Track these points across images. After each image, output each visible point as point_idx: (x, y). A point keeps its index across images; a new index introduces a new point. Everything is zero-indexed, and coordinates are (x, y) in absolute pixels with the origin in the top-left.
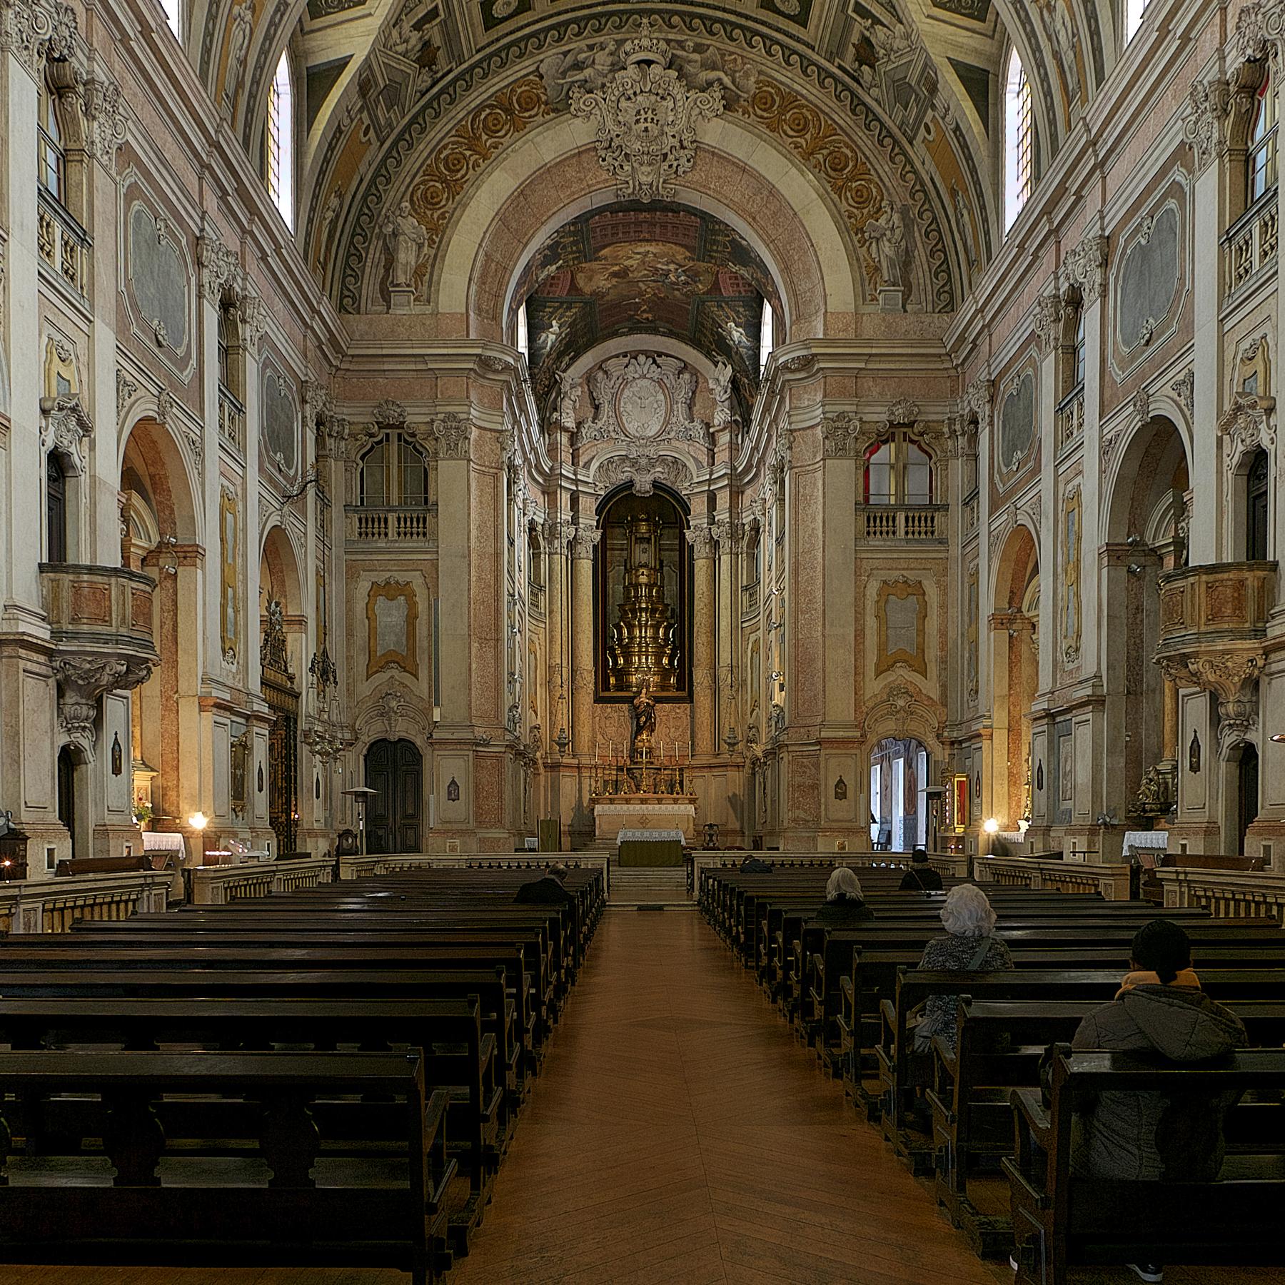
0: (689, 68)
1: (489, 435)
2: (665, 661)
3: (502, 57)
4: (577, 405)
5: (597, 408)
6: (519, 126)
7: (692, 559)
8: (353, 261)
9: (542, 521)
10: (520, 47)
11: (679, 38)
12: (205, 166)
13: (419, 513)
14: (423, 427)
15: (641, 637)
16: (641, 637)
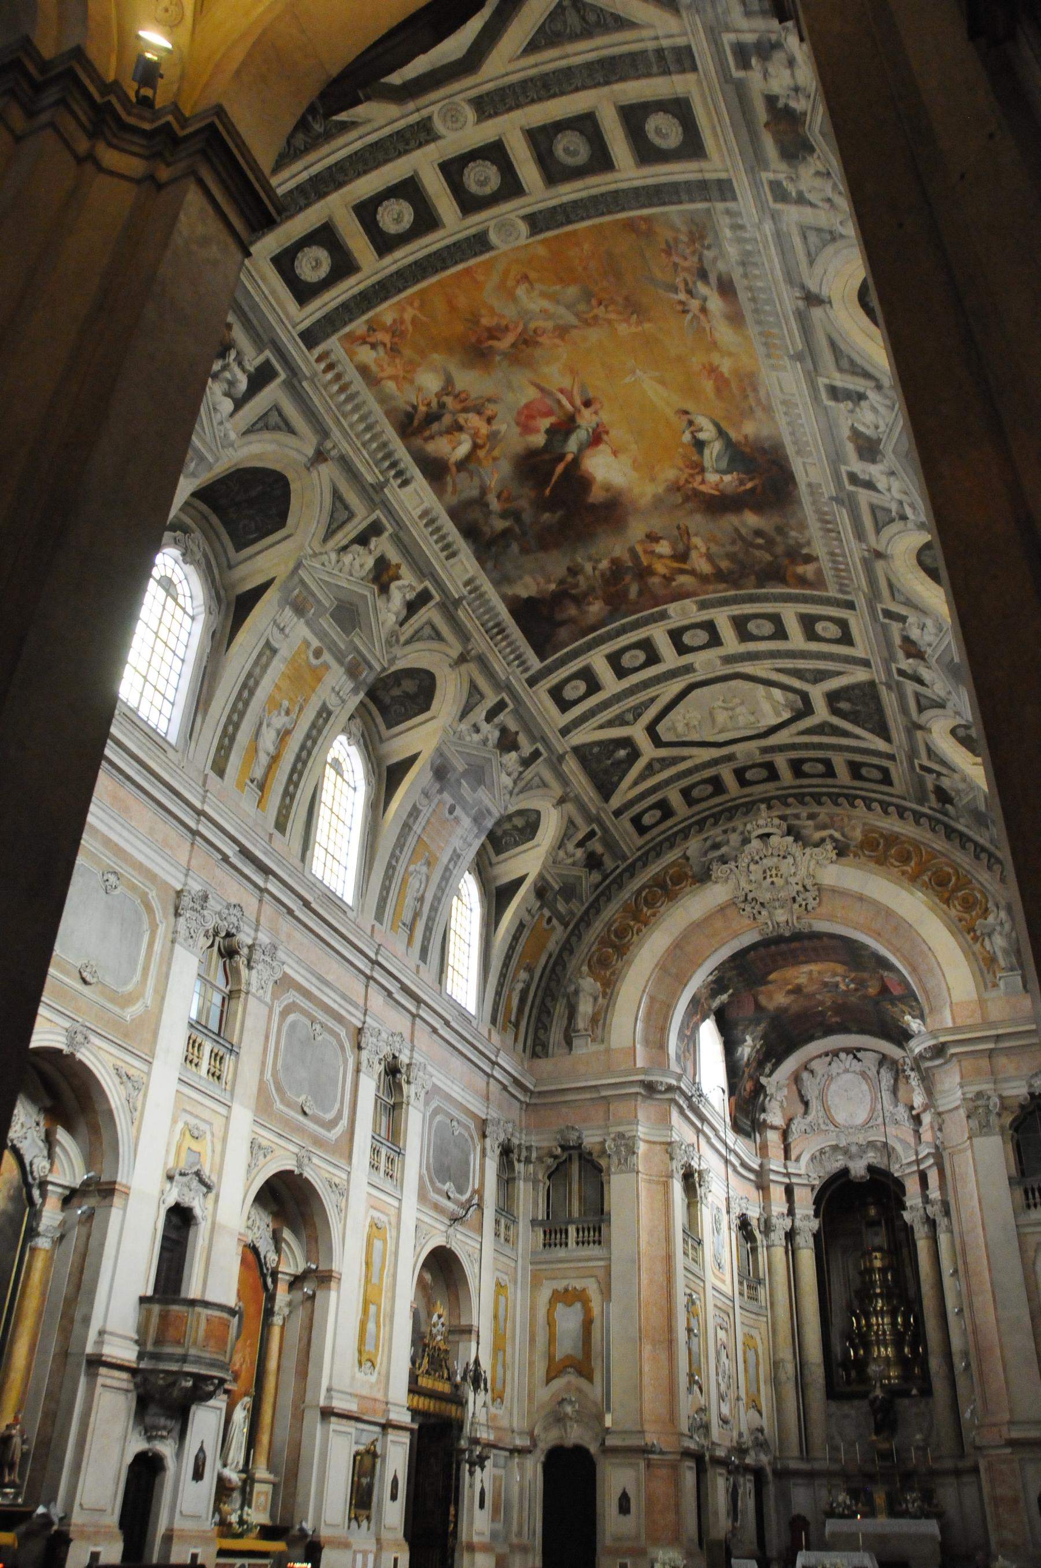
0: (805, 832)
1: (658, 1147)
3: (657, 850)
4: (785, 1104)
5: (806, 1104)
6: (671, 895)
8: (544, 1018)
9: (757, 1215)
10: (671, 842)
11: (795, 811)
12: (369, 978)
13: (596, 1223)
14: (598, 1147)
16: (878, 1325)
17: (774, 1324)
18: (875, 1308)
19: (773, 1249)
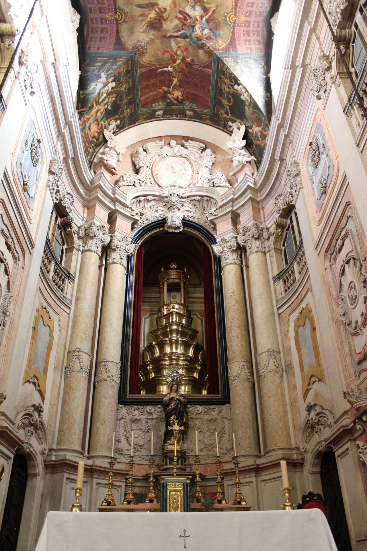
2: (196, 375)
7: (220, 269)
15: (172, 353)
17: (75, 316)
18: (171, 340)
19: (88, 253)
